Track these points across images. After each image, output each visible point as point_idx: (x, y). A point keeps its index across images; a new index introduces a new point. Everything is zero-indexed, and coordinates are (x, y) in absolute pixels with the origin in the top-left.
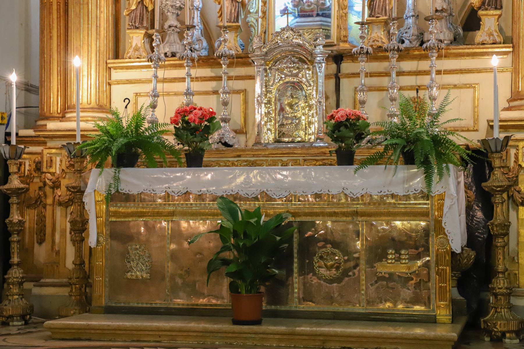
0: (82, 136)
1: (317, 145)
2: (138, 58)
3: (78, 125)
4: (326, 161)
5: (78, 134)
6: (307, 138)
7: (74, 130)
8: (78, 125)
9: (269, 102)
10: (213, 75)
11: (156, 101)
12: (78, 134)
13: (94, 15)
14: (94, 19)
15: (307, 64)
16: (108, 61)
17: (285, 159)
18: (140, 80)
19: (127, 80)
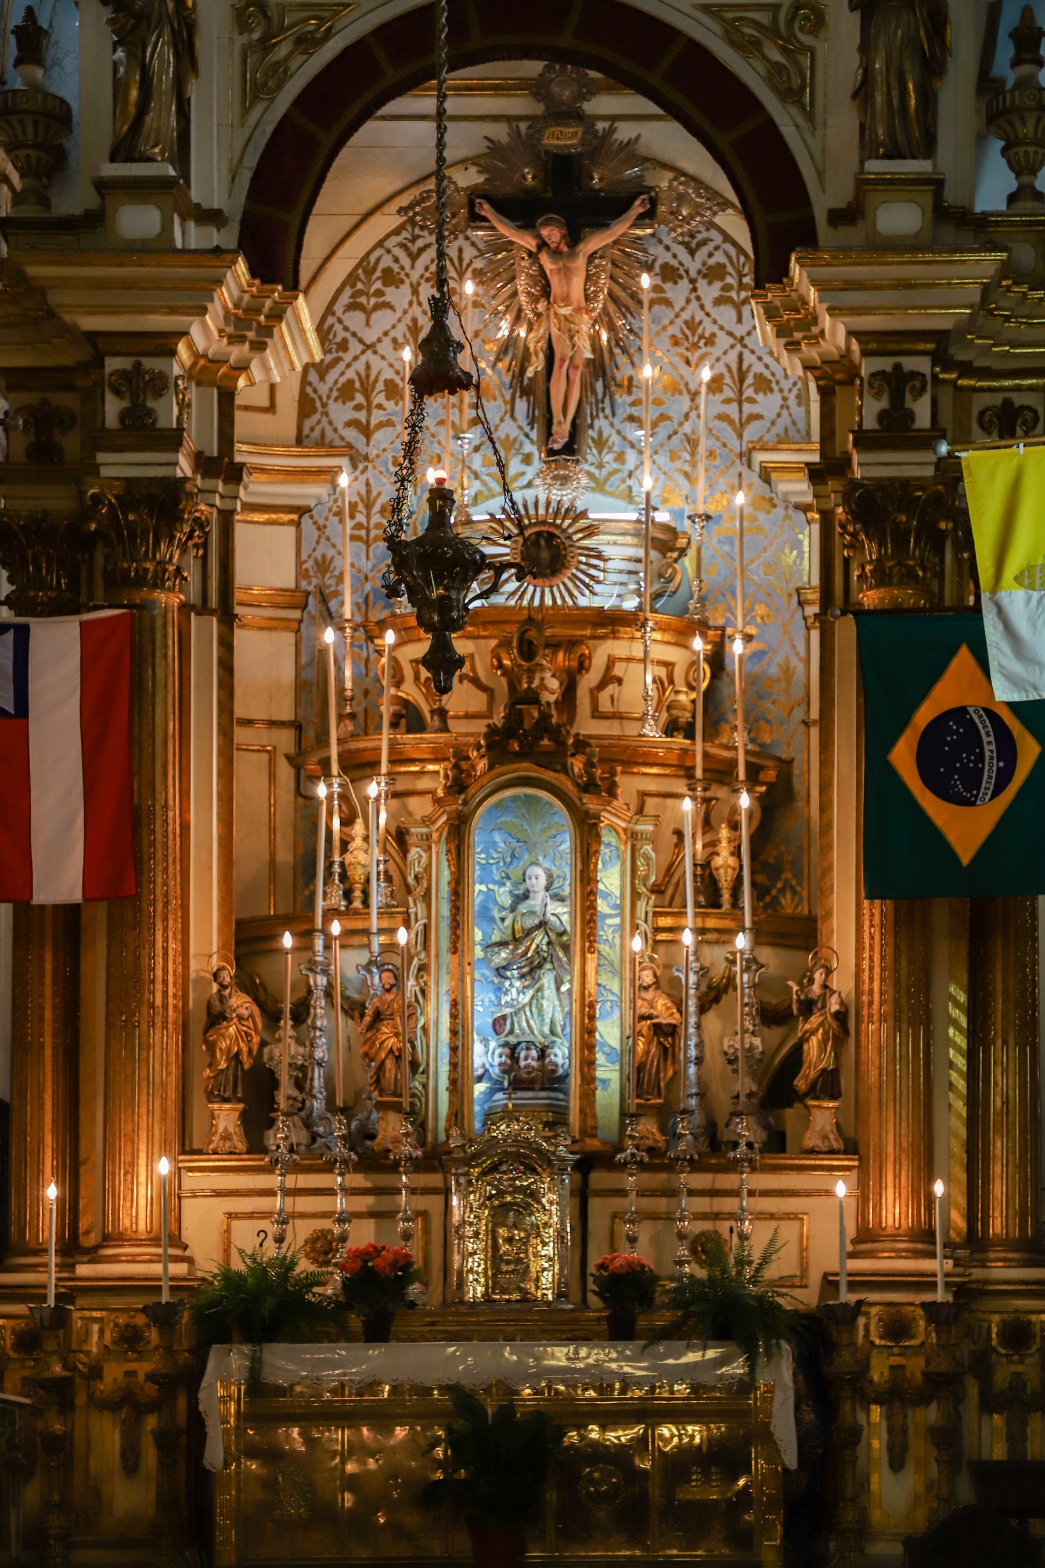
0: (172, 1288)
1: (560, 1307)
2: (231, 1153)
3: (166, 1269)
4: (578, 1333)
5: (165, 1285)
6: (539, 1294)
7: (160, 1279)
8: (166, 1269)
9: (476, 1234)
10: (368, 1184)
11: (284, 1231)
12: (165, 1285)
13: (157, 1080)
14: (158, 1087)
15: (538, 1174)
16: (181, 1157)
17: (509, 1329)
18: (237, 1191)
19: (213, 1191)
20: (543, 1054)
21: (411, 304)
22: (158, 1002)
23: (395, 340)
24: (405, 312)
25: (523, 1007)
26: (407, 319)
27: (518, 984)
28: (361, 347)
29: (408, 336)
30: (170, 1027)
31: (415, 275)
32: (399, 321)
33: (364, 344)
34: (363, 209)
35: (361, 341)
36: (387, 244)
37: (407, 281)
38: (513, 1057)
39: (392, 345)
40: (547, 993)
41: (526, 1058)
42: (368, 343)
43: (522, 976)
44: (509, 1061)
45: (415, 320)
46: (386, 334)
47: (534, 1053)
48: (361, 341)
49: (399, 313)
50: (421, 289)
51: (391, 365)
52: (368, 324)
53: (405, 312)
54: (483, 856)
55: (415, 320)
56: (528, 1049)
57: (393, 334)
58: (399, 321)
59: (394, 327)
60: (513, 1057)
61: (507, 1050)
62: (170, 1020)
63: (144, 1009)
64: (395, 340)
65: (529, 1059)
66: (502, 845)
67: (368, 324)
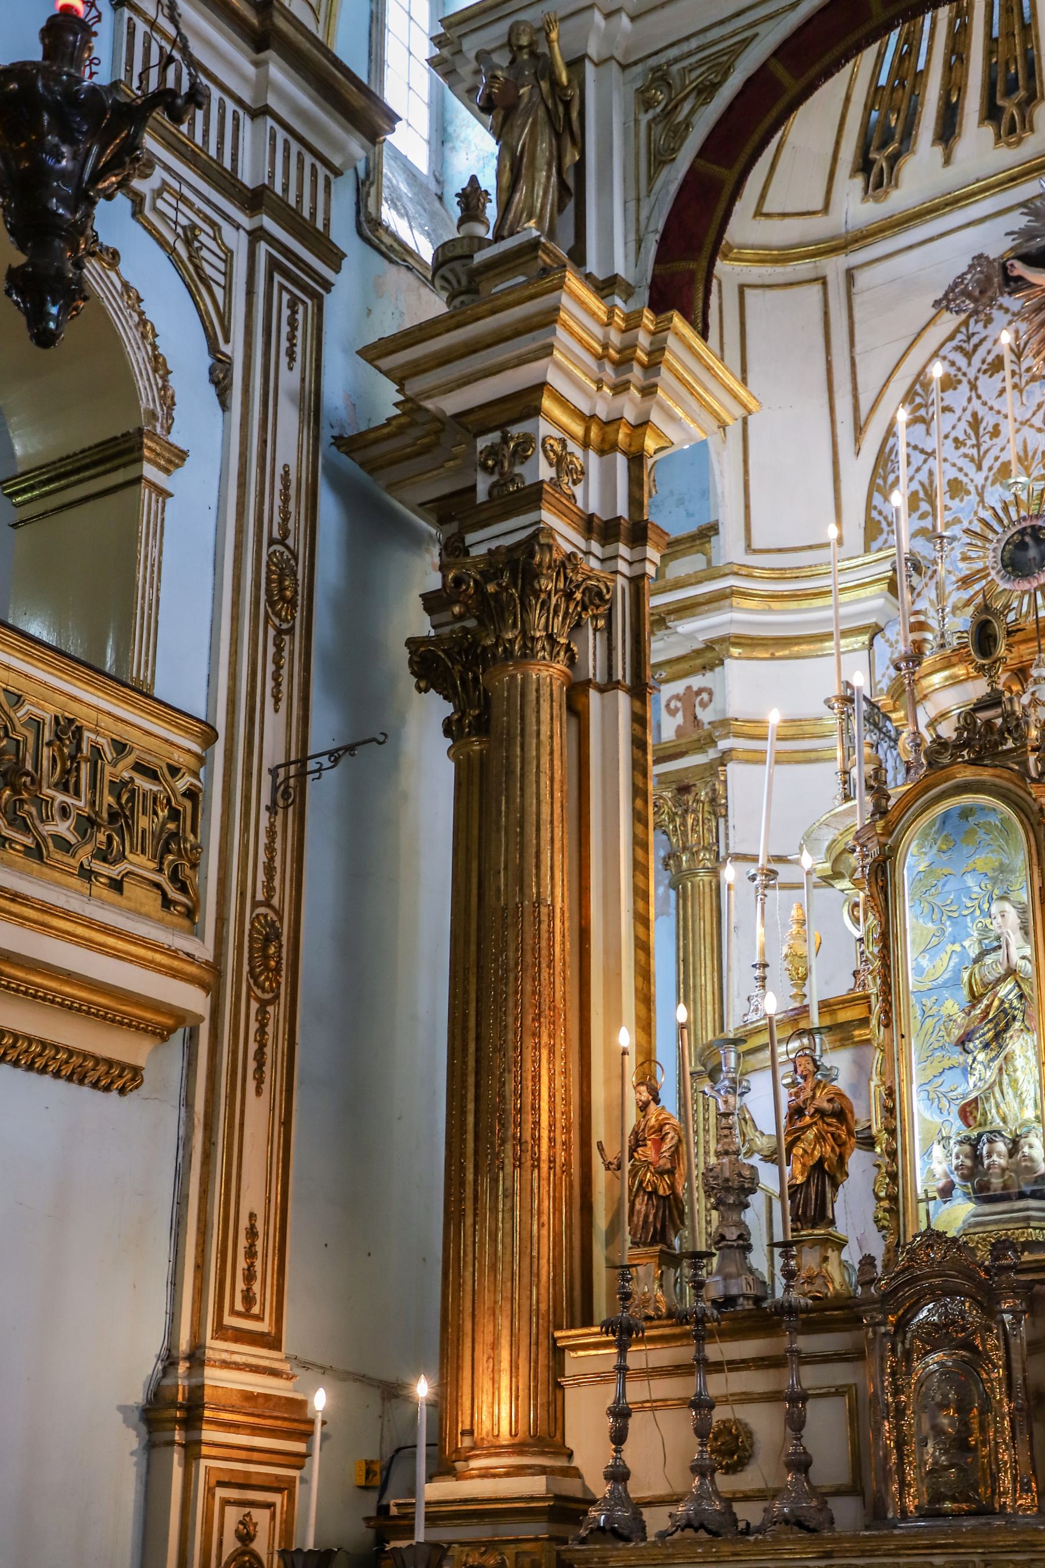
20: (1015, 1146)
21: (970, 400)
22: (527, 1136)
23: (956, 440)
24: (964, 410)
25: (991, 1087)
26: (968, 416)
27: (981, 1057)
28: (923, 457)
29: (969, 431)
30: (544, 1166)
31: (972, 373)
32: (959, 419)
33: (926, 453)
34: (916, 329)
35: (922, 451)
36: (942, 353)
37: (965, 380)
38: (976, 1157)
39: (954, 445)
40: (1019, 1062)
41: (989, 1155)
42: (929, 451)
43: (986, 1046)
44: (968, 1163)
45: (975, 415)
46: (946, 437)
47: (1001, 1147)
48: (922, 451)
49: (959, 412)
50: (979, 383)
51: (954, 465)
52: (928, 433)
53: (964, 410)
54: (954, 908)
55: (975, 415)
56: (991, 1141)
57: (953, 435)
58: (959, 419)
59: (954, 428)
60: (976, 1157)
61: (967, 1148)
62: (544, 1156)
63: (509, 1147)
64: (956, 440)
65: (998, 1155)
66: (977, 889)
67: (928, 433)
